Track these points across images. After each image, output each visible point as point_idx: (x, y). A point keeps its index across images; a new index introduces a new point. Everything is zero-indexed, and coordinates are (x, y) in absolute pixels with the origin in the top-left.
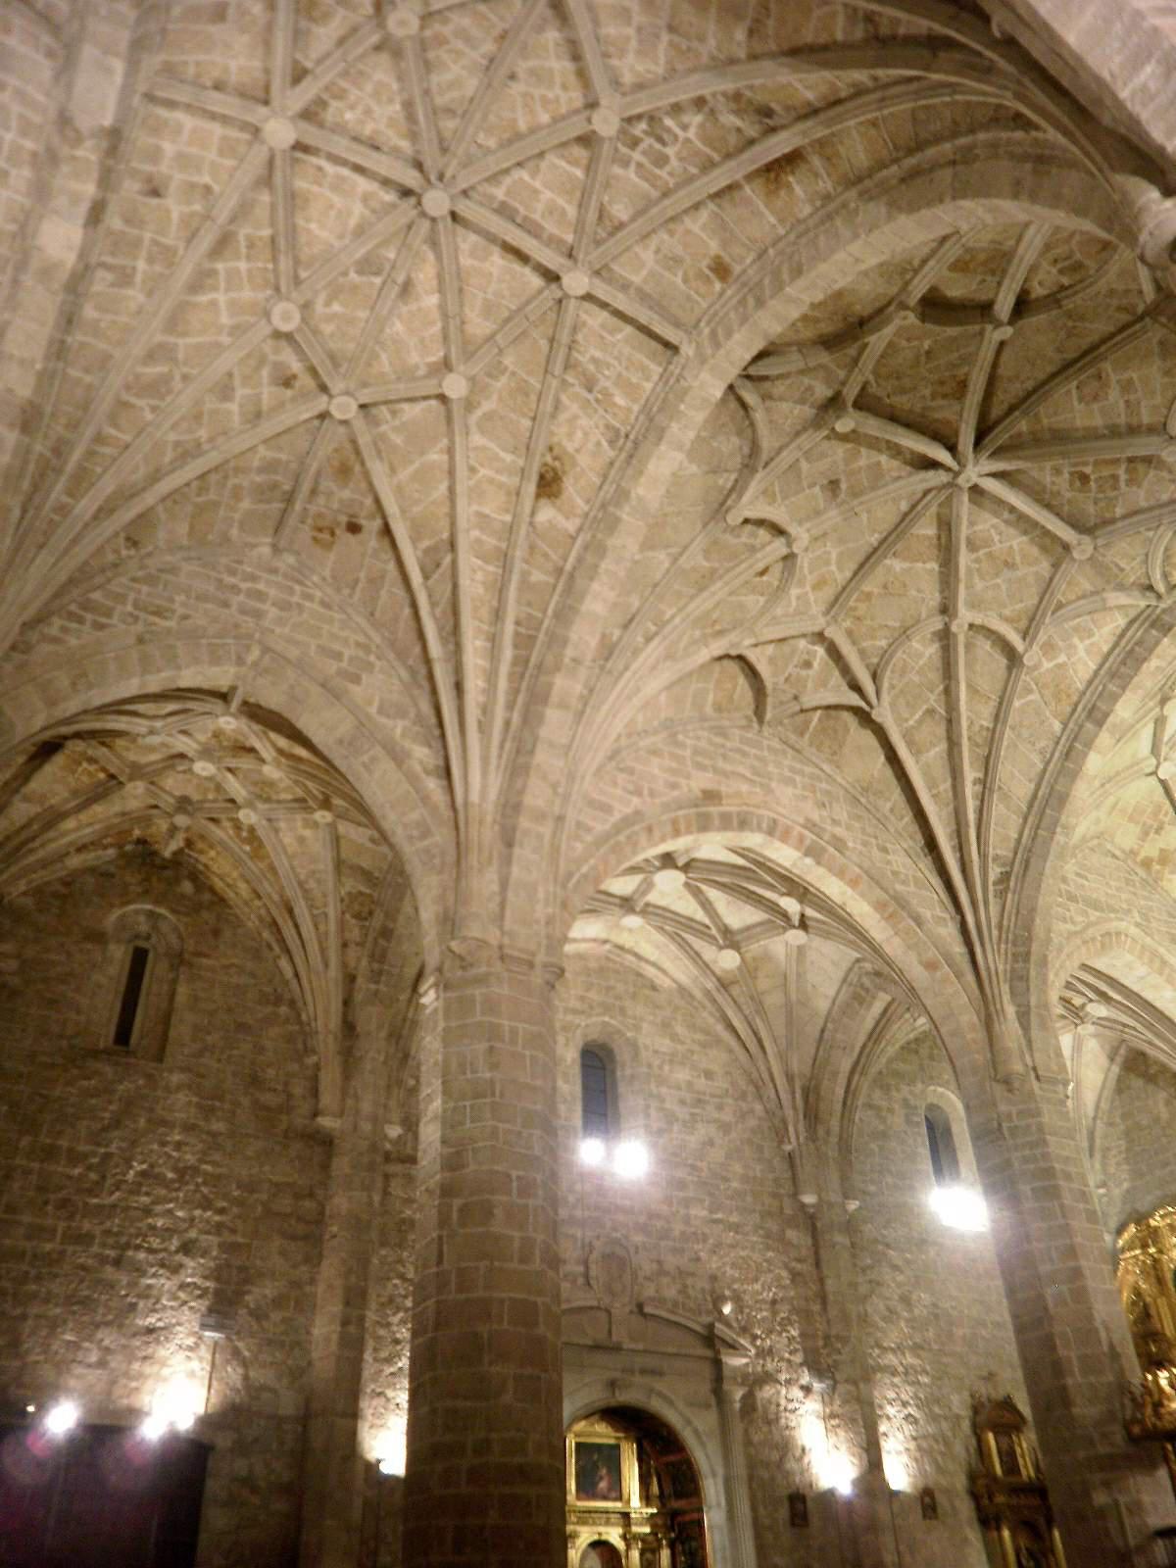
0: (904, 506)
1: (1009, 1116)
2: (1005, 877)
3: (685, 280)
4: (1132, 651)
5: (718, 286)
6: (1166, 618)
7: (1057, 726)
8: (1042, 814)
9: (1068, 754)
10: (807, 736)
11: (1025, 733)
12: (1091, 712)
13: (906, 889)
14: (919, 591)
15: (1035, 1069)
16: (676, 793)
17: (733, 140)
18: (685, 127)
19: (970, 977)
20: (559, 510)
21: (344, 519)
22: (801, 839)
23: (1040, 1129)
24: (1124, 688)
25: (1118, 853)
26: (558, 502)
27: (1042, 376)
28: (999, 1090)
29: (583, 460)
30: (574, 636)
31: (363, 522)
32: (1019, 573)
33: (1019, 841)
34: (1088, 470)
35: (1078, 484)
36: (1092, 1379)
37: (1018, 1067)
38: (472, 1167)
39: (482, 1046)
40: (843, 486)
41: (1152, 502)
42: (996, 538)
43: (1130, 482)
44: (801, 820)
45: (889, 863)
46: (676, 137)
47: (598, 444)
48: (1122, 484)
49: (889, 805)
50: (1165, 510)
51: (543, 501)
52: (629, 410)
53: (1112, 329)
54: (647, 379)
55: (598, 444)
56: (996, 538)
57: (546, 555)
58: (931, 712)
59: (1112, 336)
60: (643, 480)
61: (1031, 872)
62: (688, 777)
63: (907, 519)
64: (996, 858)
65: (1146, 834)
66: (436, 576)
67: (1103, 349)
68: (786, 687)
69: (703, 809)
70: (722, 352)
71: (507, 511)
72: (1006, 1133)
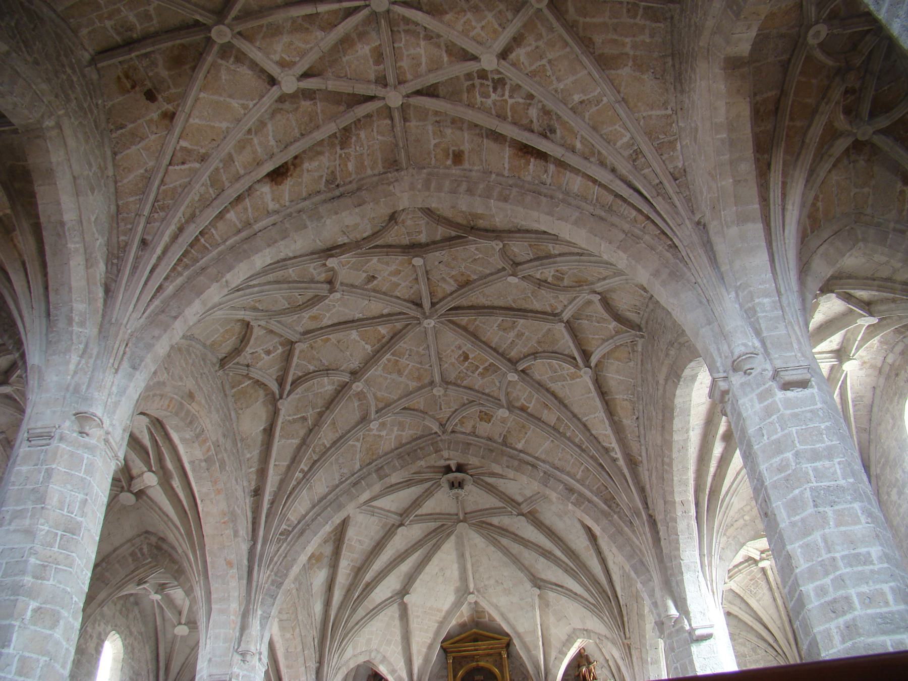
0: (385, 312)
1: (238, 675)
2: (286, 533)
3: (436, 145)
4: (416, 450)
5: (449, 162)
6: (440, 444)
7: (357, 466)
8: (326, 508)
9: (355, 484)
10: (235, 390)
11: (341, 460)
12: (379, 469)
13: (239, 512)
14: (351, 355)
16: (180, 384)
17: (525, 121)
18: (511, 97)
19: (245, 582)
20: (272, 192)
21: (149, 85)
22: (209, 450)
24: (402, 467)
26: (275, 187)
27: (497, 303)
28: (237, 657)
29: (306, 178)
30: (236, 270)
31: (160, 98)
32: (401, 379)
33: (304, 516)
34: (471, 356)
35: (462, 358)
38: (51, 582)
39: (81, 496)
40: (375, 282)
41: (481, 390)
42: (407, 356)
43: (481, 374)
44: (214, 439)
45: (236, 490)
46: (503, 95)
47: (321, 176)
48: (477, 372)
49: (248, 456)
50: (484, 397)
51: (267, 180)
52: (350, 174)
53: (539, 309)
54: (372, 169)
55: (321, 176)
56: (407, 356)
57: (246, 209)
58: (304, 419)
59: (537, 312)
60: (334, 217)
61: (303, 539)
62: (187, 377)
63: (382, 318)
64: (288, 520)
66: (176, 167)
67: (529, 314)
68: (249, 357)
69: (183, 401)
70: (427, 193)
71: (245, 168)
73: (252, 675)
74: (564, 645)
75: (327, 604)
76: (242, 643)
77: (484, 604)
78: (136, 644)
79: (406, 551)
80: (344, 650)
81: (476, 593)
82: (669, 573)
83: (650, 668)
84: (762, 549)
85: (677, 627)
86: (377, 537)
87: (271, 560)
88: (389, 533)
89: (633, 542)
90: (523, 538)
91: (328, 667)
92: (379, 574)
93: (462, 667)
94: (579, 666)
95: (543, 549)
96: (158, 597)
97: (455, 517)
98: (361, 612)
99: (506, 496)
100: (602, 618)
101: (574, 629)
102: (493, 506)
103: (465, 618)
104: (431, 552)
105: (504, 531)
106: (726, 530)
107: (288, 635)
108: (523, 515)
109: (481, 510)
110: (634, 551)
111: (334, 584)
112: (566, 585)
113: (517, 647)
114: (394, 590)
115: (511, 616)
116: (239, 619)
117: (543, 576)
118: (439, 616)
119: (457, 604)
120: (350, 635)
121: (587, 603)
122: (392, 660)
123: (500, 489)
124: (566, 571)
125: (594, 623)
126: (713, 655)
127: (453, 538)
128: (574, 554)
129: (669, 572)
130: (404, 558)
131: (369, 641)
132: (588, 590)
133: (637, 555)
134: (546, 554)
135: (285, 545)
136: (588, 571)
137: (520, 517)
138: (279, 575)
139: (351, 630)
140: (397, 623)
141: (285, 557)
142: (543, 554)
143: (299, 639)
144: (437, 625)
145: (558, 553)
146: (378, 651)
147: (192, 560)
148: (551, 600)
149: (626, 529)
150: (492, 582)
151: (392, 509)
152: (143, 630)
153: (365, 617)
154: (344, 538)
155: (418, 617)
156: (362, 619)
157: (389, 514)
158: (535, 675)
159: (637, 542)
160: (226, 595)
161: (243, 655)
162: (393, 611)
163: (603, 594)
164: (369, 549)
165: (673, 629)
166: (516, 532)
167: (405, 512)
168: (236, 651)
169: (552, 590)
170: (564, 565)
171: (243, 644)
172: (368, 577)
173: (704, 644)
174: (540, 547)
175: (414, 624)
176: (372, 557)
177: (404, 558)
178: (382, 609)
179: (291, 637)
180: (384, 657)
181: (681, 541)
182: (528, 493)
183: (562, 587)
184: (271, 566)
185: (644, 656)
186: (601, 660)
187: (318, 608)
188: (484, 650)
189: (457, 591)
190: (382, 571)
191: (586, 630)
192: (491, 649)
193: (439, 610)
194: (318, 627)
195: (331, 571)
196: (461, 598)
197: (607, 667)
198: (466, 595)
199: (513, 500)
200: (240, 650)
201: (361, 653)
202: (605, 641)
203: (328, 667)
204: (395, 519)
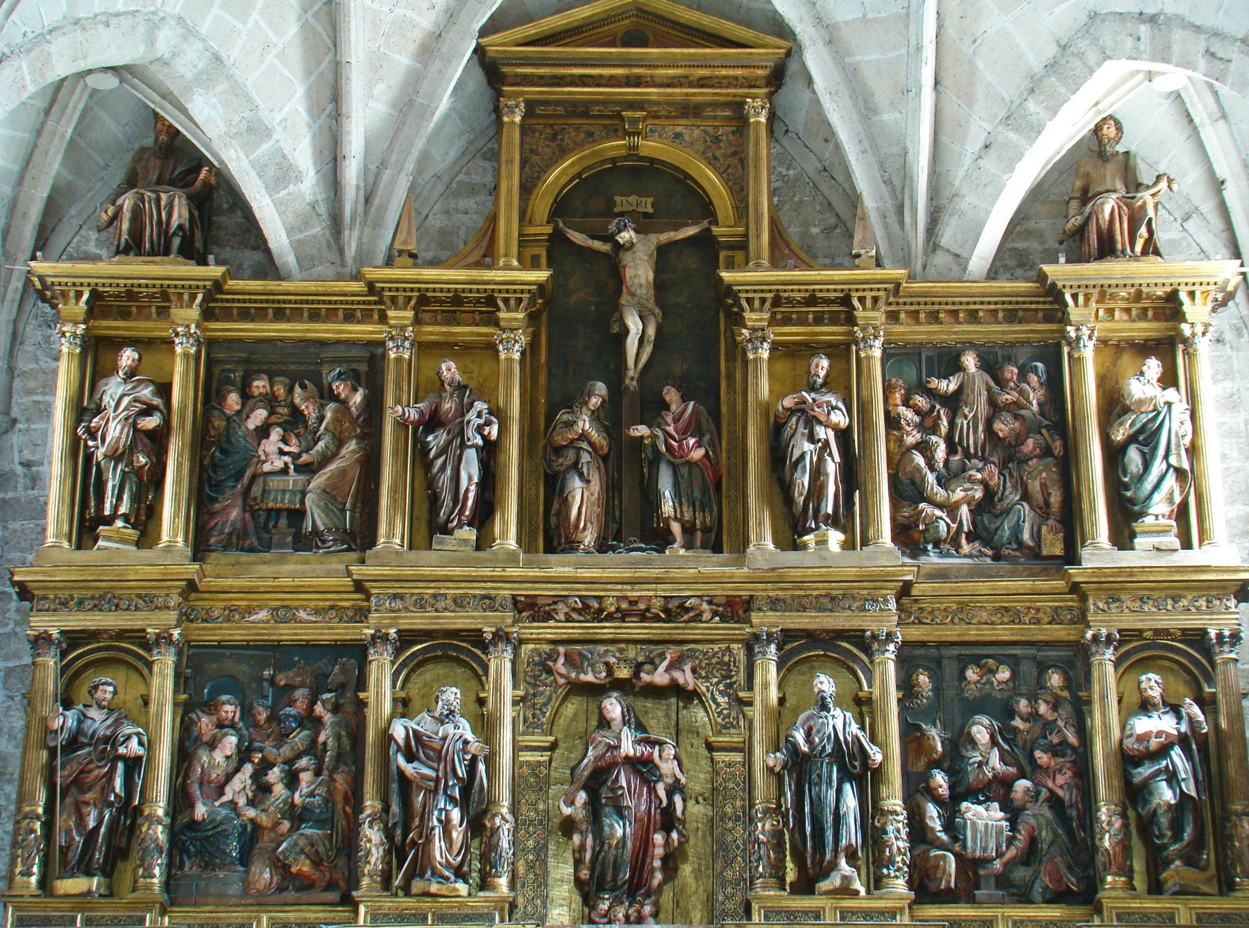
93: (563, 153)
94: (1086, 196)
101: (1093, 16)
122: (250, 80)
146: (188, 31)
180: (217, 58)
186: (1191, 183)
191: (1153, 19)
192: (702, 82)
197: (1216, 222)
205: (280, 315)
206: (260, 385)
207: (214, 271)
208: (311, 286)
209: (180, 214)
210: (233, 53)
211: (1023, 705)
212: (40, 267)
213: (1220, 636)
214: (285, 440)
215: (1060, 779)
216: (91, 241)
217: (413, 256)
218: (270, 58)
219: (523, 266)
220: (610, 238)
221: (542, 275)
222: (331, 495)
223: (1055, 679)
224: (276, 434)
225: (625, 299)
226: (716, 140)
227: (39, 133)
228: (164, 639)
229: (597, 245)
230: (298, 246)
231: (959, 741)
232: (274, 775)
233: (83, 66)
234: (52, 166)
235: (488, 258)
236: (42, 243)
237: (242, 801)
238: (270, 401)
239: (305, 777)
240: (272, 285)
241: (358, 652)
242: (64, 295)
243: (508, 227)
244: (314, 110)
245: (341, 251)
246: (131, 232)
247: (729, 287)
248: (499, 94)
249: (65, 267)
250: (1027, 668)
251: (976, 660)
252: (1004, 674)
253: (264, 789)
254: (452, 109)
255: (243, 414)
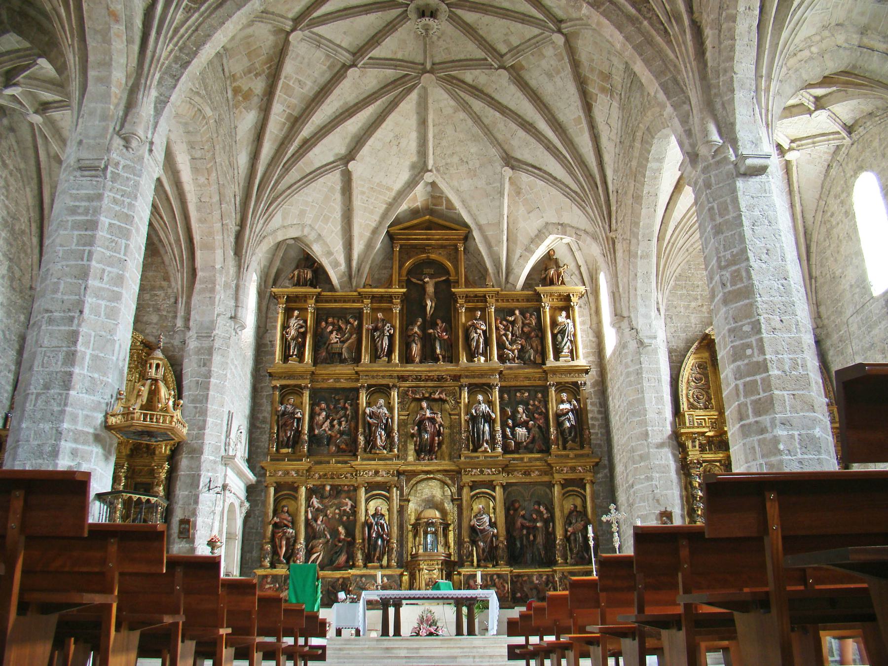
1: (117, 164)
15: (152, 143)
19: (136, 48)
23: (136, 185)
25: (226, 70)
28: (118, 142)
36: (96, 376)
37: (141, 132)
65: (250, 72)
72: (109, 175)
73: (138, 167)
74: (532, 241)
75: (255, 157)
76: (126, 124)
77: (442, 185)
78: (12, 180)
79: (357, 104)
80: (271, 216)
81: (435, 172)
82: (713, 92)
83: (640, 262)
84: (793, 138)
85: (718, 158)
86: (322, 80)
87: (176, 31)
88: (338, 76)
89: (667, 55)
90: (499, 103)
91: (251, 231)
92: (321, 130)
93: (410, 258)
94: (546, 269)
95: (523, 119)
96: (37, 119)
97: (420, 67)
98: (294, 174)
99: (488, 43)
100: (584, 208)
101: (547, 223)
102: (469, 57)
103: (419, 203)
104: (387, 110)
105: (477, 91)
106: (788, 59)
107: (202, 180)
108: (504, 68)
109: (453, 61)
110: (666, 65)
111: (264, 133)
112: (544, 168)
113: (477, 240)
114: (337, 155)
115: (473, 204)
116: (125, 96)
117: (519, 156)
118: (389, 196)
119: (411, 184)
120: (280, 200)
121: (568, 190)
122: (328, 240)
123: (481, 32)
124: (548, 148)
125: (575, 216)
126: (764, 195)
127: (414, 95)
128: (561, 127)
129: (713, 91)
130: (353, 112)
131: (302, 213)
132: (571, 173)
133: (670, 71)
134: (528, 127)
135: (196, 15)
136: (575, 149)
137: (501, 71)
138: (186, 52)
139: (281, 195)
140: (338, 196)
141: (196, 30)
142: (523, 125)
143: (216, 186)
144: (385, 206)
145: (543, 126)
146: (312, 228)
147: (64, 15)
148: (523, 187)
149: (659, 39)
150: (455, 159)
151: (343, 45)
152: (22, 166)
153: (299, 181)
154: (280, 71)
155: (363, 193)
156: (295, 183)
157: (339, 50)
158: (494, 274)
159: (671, 55)
160: (107, 58)
161: (127, 141)
162: (334, 179)
163: (590, 178)
164: (311, 94)
165: (712, 161)
166: (494, 95)
167: (359, 50)
168: (118, 133)
169: (527, 172)
170: (546, 141)
171: (127, 126)
172: (307, 131)
173: (754, 181)
174: (519, 116)
175: (358, 202)
176: (313, 104)
177: (353, 112)
178: (321, 175)
179: (206, 182)
180: (320, 235)
181: (737, 48)
182: (515, 41)
183: (539, 169)
184: (175, 39)
185: (632, 248)
186: (572, 266)
187: (243, 160)
188: (438, 240)
189: (413, 167)
190: (325, 127)
191: (562, 225)
192: (447, 240)
193: (389, 189)
194: (241, 185)
195: (262, 116)
196: (416, 176)
197: (579, 277)
198: (422, 174)
199: (495, 50)
200: (123, 131)
201: (292, 226)
202: (584, 236)
203: (251, 231)
204: (346, 58)
205: (335, 301)
206: (330, 320)
207: (319, 290)
208: (344, 294)
209: (309, 275)
210: (324, 233)
211: (531, 402)
212: (274, 290)
213: (581, 383)
214: (337, 334)
215: (541, 421)
216: (287, 283)
217: (370, 285)
218: (333, 234)
219: (400, 288)
220: (422, 280)
221: (404, 290)
222: (349, 349)
223: (540, 395)
224: (335, 333)
225: (426, 296)
226: (450, 254)
227: (274, 255)
228: (306, 387)
229: (419, 282)
230: (340, 283)
231: (515, 412)
232: (335, 422)
233: (285, 238)
234: (277, 264)
235: (390, 285)
236: (275, 284)
237: (327, 429)
238: (333, 324)
239: (343, 423)
240: (334, 294)
241: (357, 390)
242: (280, 297)
243: (395, 277)
244: (345, 248)
245: (351, 284)
246: (297, 280)
247: (454, 293)
248: (393, 243)
249: (280, 290)
250: (532, 392)
251: (519, 391)
252: (527, 394)
253: (332, 426)
254: (380, 247)
255: (326, 328)
